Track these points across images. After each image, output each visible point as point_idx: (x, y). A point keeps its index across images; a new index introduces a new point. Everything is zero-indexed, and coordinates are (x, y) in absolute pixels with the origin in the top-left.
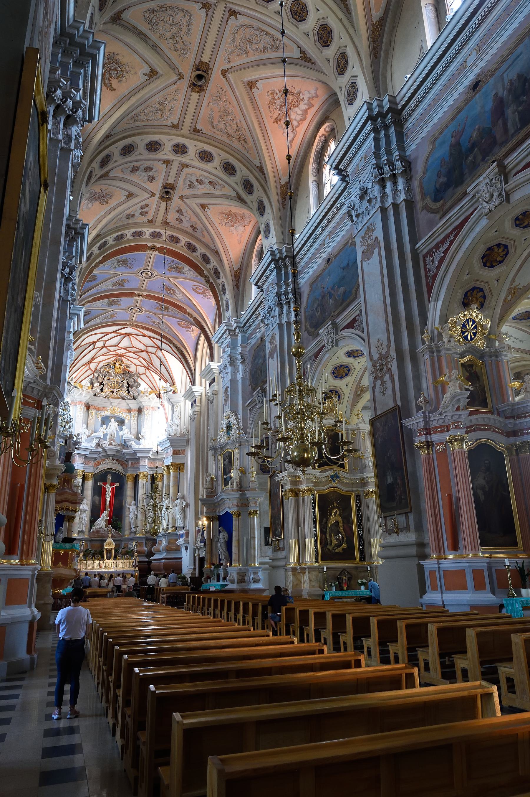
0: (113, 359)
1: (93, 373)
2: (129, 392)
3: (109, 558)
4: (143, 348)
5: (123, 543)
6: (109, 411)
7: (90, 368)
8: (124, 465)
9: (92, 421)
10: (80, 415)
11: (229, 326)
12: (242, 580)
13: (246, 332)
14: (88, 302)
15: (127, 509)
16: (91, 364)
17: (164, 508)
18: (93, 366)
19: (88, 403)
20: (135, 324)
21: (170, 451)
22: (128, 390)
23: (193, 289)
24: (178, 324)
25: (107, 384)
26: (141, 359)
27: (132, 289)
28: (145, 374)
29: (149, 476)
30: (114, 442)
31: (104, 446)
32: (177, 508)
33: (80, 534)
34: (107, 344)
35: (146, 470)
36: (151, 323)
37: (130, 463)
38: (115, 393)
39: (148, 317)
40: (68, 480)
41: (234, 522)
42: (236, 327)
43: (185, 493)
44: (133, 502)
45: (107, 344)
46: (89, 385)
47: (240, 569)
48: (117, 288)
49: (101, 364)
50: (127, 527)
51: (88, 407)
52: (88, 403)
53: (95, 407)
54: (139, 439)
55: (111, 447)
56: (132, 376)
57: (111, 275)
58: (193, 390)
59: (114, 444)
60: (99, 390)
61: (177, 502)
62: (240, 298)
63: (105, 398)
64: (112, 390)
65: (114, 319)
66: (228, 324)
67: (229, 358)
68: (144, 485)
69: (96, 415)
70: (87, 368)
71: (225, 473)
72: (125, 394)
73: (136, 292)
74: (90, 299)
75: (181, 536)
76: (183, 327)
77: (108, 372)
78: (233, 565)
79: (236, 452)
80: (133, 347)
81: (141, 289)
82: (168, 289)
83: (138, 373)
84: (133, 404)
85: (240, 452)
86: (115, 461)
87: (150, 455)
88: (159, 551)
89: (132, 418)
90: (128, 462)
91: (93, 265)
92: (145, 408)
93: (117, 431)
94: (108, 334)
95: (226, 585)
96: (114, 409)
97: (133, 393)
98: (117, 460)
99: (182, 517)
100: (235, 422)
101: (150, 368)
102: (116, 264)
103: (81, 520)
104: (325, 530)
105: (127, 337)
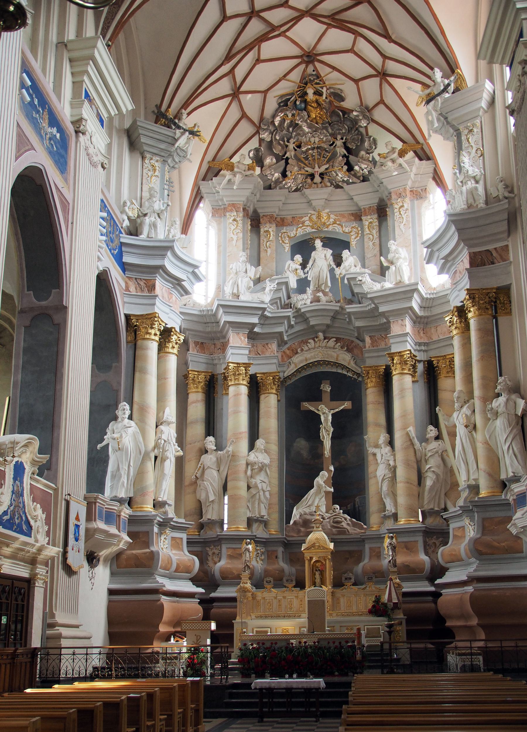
0: (296, 76)
1: (257, 132)
2: (350, 169)
6: (307, 223)
7: (244, 115)
8: (356, 351)
10: (235, 238)
15: (371, 458)
19: (255, 211)
22: (348, 163)
25: (295, 156)
28: (382, 102)
29: (420, 367)
30: (325, 294)
35: (409, 348)
38: (317, 179)
44: (383, 437)
52: (255, 211)
53: (271, 217)
55: (316, 306)
59: (323, 298)
64: (310, 170)
69: (277, 236)
72: (341, 175)
77: (294, 125)
83: (367, 108)
86: (332, 343)
89: (367, 231)
90: (363, 341)
93: (332, 271)
96: (319, 217)
98: (338, 340)
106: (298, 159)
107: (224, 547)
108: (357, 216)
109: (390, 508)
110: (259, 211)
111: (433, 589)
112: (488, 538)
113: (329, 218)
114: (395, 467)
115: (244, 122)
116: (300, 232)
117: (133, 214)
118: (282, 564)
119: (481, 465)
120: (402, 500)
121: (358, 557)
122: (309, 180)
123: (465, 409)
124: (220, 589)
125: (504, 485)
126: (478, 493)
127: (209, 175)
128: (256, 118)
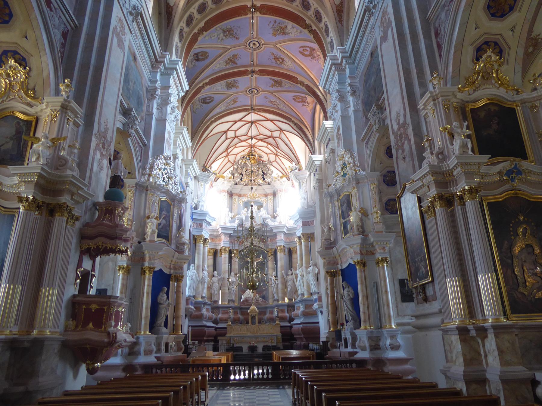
0: (247, 151)
2: (264, 179)
3: (253, 323)
4: (269, 133)
5: (268, 310)
6: (249, 196)
7: (229, 161)
9: (235, 206)
11: (334, 60)
12: (375, 346)
13: (354, 63)
14: (207, 84)
16: (229, 156)
17: (299, 276)
18: (231, 158)
20: (256, 108)
21: (300, 224)
22: (263, 178)
23: (300, 52)
24: (294, 99)
26: (269, 146)
27: (244, 66)
28: (275, 161)
29: (286, 250)
31: (246, 226)
32: (310, 275)
33: (230, 302)
34: (239, 133)
36: (270, 104)
37: (269, 239)
39: (266, 97)
40: (112, 210)
41: (358, 275)
42: (343, 58)
43: (317, 261)
45: (239, 133)
46: (230, 175)
47: (372, 332)
48: (231, 66)
49: (239, 157)
50: (270, 296)
51: (231, 195)
54: (275, 217)
56: (265, 165)
57: (221, 51)
58: (313, 159)
60: (239, 180)
61: (310, 269)
62: (345, 32)
63: (245, 185)
65: (237, 104)
66: (332, 58)
67: (337, 94)
68: (281, 257)
69: (238, 201)
70: (226, 160)
71: (344, 218)
72: (261, 181)
73: (249, 69)
74: (207, 81)
75: (315, 301)
76: (298, 102)
77: (245, 163)
78: (363, 327)
79: (354, 192)
80: (260, 134)
81: (252, 65)
82: (277, 59)
83: (270, 161)
84: (268, 189)
85: (358, 191)
87: (285, 231)
88: (297, 316)
91: (196, 31)
92: (278, 191)
94: (236, 122)
95: (356, 353)
97: (268, 180)
99: (315, 283)
100: (351, 160)
101: (278, 154)
102: (222, 35)
103: (230, 290)
104: (509, 261)
105: (274, 155)
106: (246, 175)
107: (220, 310)
108: (266, 195)
109: (276, 297)
110: (233, 192)
111: (290, 325)
112: (306, 310)
113: (256, 195)
114: (278, 284)
115: (229, 163)
116: (246, 199)
117: (196, 201)
118: (240, 316)
119: (305, 288)
120: (280, 295)
121: (265, 313)
122: (250, 182)
123: (300, 270)
124: (219, 325)
125: (312, 294)
126: (304, 296)
127: (216, 180)
128: (232, 162)
